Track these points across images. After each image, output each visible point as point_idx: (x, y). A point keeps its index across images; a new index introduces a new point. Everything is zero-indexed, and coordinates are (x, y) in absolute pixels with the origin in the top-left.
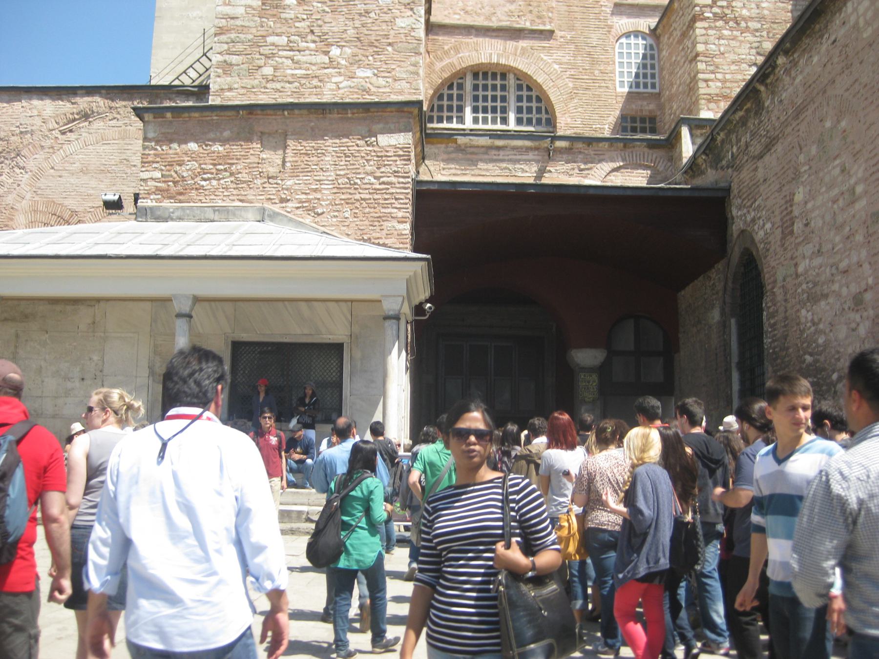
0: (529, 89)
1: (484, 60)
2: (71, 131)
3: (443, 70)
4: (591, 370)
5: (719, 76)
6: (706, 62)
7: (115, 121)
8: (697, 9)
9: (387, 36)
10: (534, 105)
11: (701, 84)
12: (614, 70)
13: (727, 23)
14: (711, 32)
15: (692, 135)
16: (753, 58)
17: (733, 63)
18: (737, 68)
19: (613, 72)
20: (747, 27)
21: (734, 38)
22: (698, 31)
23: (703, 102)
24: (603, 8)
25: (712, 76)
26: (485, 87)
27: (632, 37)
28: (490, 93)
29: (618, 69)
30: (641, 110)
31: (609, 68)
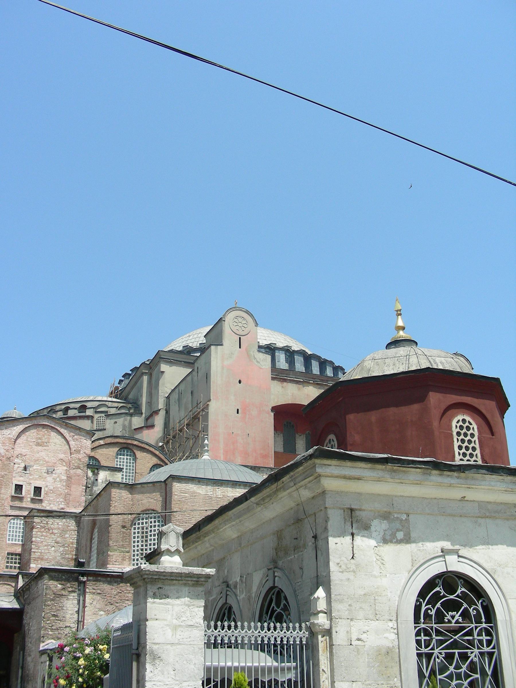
5: (40, 551)
6: (35, 545)
8: (34, 524)
12: (7, 533)
13: (45, 530)
14: (39, 533)
16: (53, 544)
17: (46, 546)
18: (47, 548)
19: (6, 534)
20: (53, 532)
22: (34, 533)
23: (32, 560)
24: (5, 507)
25: (37, 551)
27: (16, 519)
29: (8, 533)
30: (16, 551)
31: (5, 533)
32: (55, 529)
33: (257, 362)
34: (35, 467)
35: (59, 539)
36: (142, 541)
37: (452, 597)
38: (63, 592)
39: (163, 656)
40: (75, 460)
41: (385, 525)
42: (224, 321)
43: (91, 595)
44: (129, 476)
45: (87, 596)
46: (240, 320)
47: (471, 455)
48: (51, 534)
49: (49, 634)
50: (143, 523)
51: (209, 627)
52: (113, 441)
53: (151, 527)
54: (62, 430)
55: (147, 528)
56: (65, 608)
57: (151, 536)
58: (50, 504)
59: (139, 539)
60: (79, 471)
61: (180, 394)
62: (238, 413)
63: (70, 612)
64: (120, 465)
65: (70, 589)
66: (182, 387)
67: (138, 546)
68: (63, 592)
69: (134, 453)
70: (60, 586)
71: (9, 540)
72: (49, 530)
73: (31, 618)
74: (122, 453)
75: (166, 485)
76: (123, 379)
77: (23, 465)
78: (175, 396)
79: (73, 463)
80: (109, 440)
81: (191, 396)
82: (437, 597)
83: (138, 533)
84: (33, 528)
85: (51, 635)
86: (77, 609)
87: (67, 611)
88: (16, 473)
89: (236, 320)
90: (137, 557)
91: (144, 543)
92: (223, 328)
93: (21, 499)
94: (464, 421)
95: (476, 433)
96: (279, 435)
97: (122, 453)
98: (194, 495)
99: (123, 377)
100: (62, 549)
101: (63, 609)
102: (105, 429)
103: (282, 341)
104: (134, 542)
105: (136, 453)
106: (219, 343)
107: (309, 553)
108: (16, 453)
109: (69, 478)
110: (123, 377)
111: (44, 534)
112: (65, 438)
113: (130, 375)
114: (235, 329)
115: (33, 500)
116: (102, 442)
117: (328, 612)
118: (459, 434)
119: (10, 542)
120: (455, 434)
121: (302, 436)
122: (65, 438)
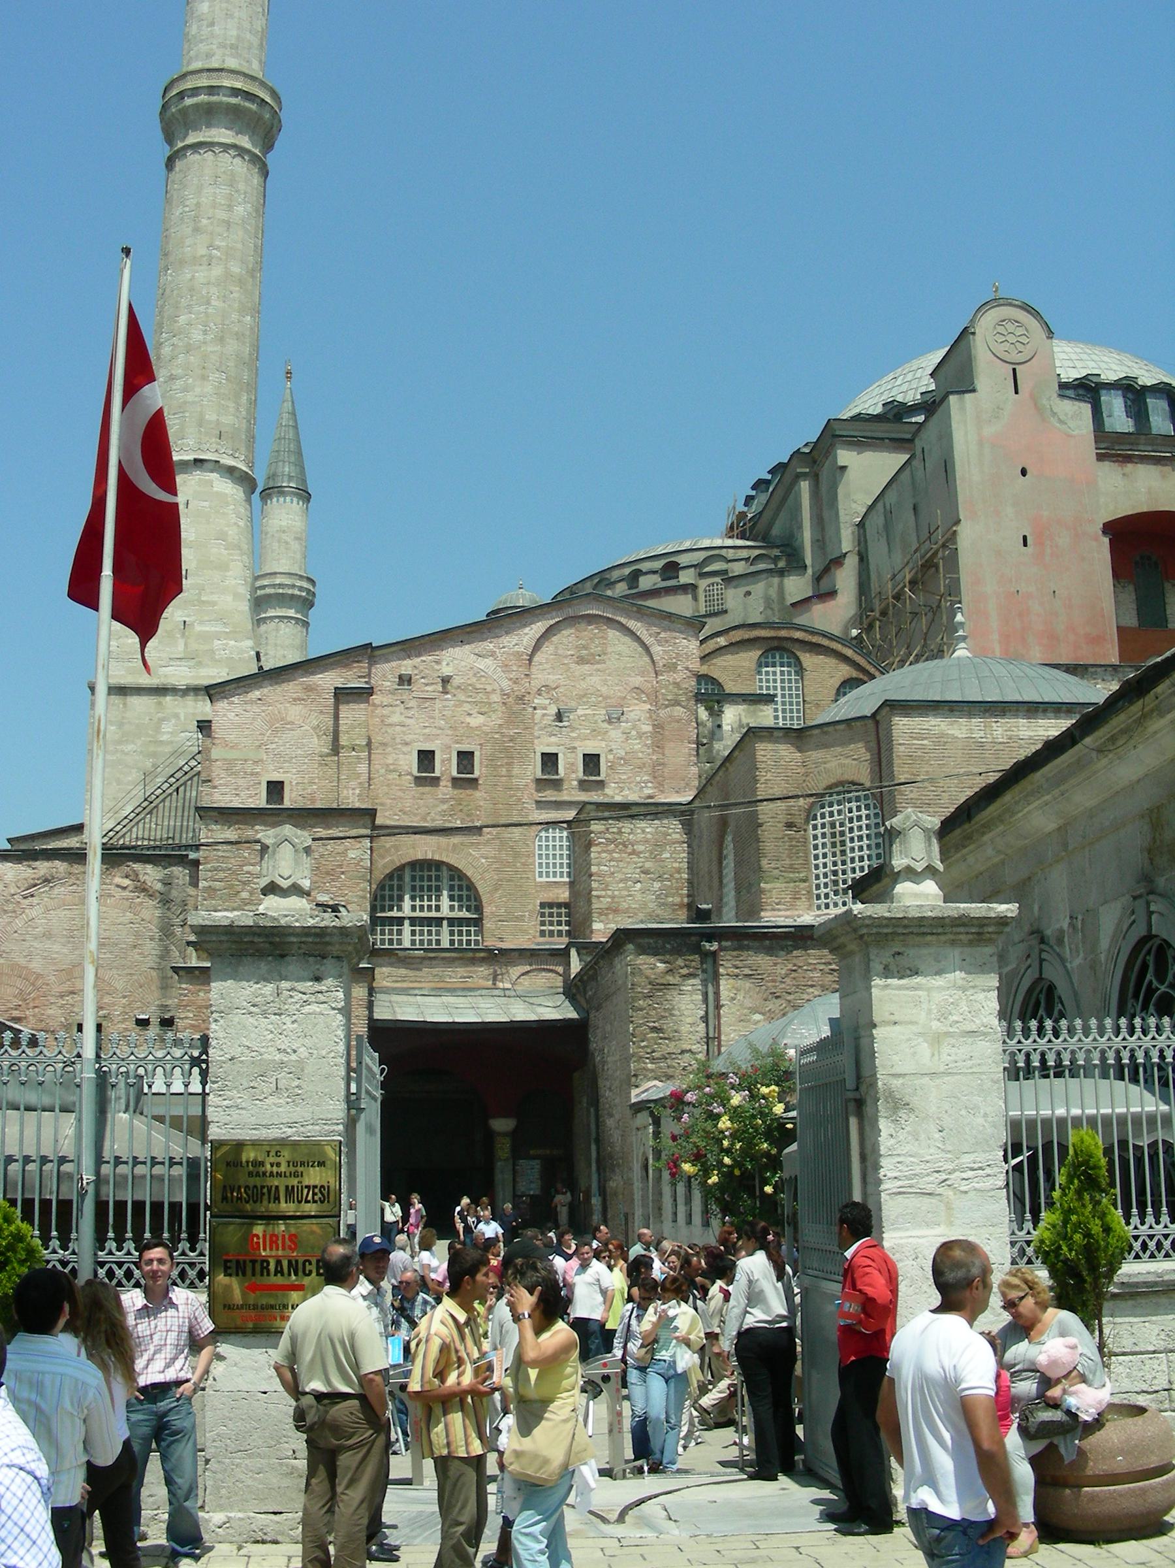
0: (460, 879)
1: (420, 857)
2: (32, 896)
3: (385, 867)
4: (505, 1134)
5: (609, 893)
7: (75, 887)
9: (341, 866)
10: (464, 893)
11: (594, 900)
13: (617, 846)
14: (604, 855)
15: (579, 954)
22: (592, 855)
25: (603, 893)
26: (422, 879)
28: (425, 884)
29: (538, 861)
32: (638, 843)
33: (1061, 421)
34: (580, 712)
35: (648, 865)
36: (834, 855)
38: (670, 979)
39: (915, 1101)
40: (666, 687)
42: (974, 333)
43: (731, 981)
44: (791, 711)
45: (722, 982)
46: (1011, 327)
48: (630, 854)
49: (647, 1070)
50: (831, 814)
51: (1010, 1033)
52: (746, 637)
53: (851, 820)
54: (632, 624)
55: (842, 825)
56: (676, 1012)
57: (852, 840)
58: (622, 789)
59: (826, 850)
60: (679, 711)
61: (888, 514)
62: (1025, 544)
63: (689, 1020)
64: (768, 688)
65: (685, 971)
66: (891, 497)
67: (825, 866)
68: (670, 979)
69: (798, 659)
70: (661, 966)
71: (541, 876)
72: (626, 846)
73: (606, 1038)
74: (770, 660)
75: (877, 723)
76: (753, 493)
77: (553, 710)
78: (877, 520)
79: (663, 694)
80: (737, 636)
83: (824, 835)
84: (589, 845)
85: (652, 1071)
86: (702, 1013)
87: (682, 1018)
88: (541, 729)
89: (1000, 329)
90: (826, 891)
91: (838, 859)
92: (973, 352)
93: (557, 784)
96: (1124, 587)
97: (770, 660)
98: (941, 740)
99: (753, 488)
100: (657, 885)
101: (673, 1015)
102: (726, 612)
103: (1115, 367)
104: (816, 857)
105: (801, 658)
106: (966, 386)
108: (536, 684)
109: (658, 727)
110: (753, 488)
111: (616, 855)
112: (638, 639)
113: (767, 482)
114: (1000, 350)
115: (583, 785)
116: (722, 641)
119: (544, 879)
122: (638, 639)
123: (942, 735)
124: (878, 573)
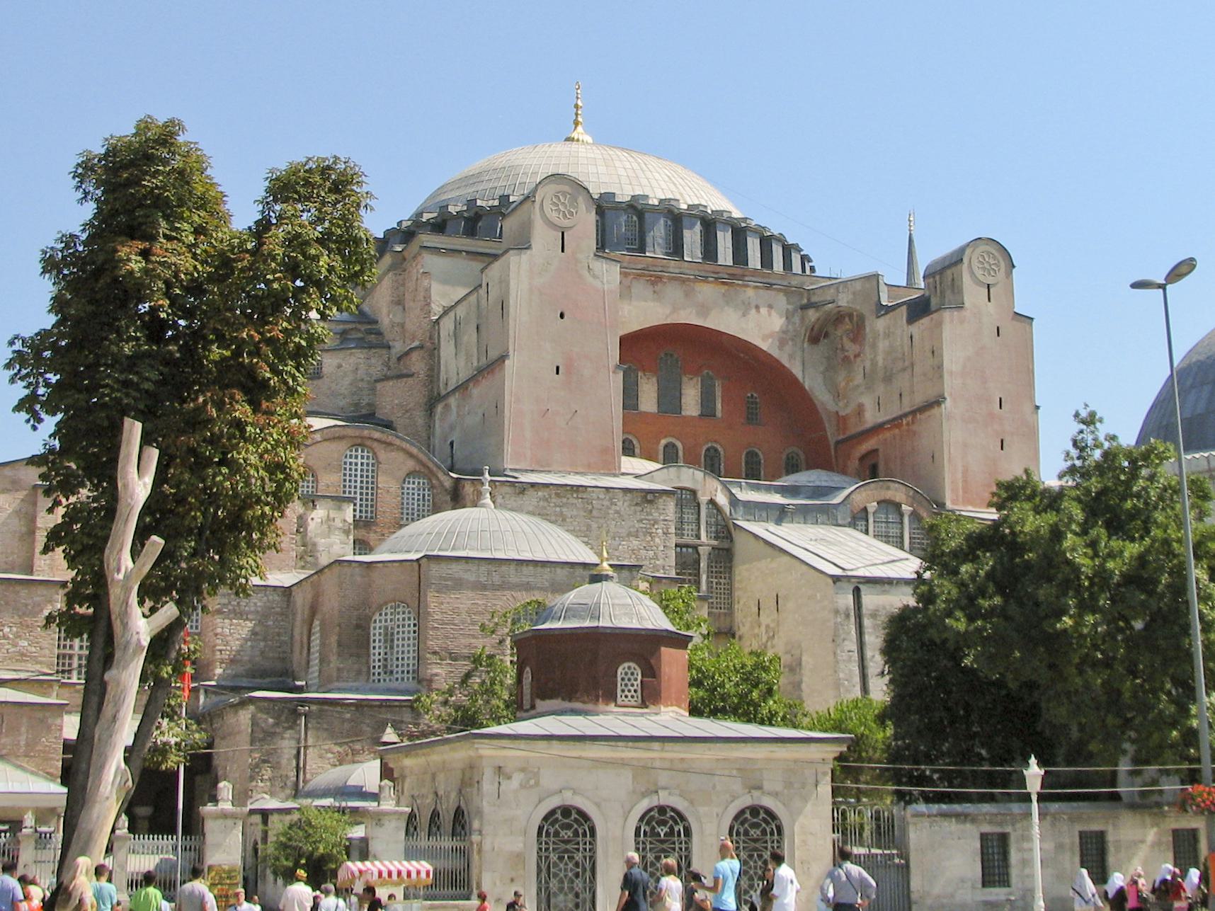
21: (240, 625)
36: (386, 648)
37: (567, 821)
38: (278, 730)
41: (522, 775)
47: (632, 697)
61: (457, 324)
62: (558, 373)
70: (271, 720)
74: (354, 453)
75: (420, 565)
81: (475, 335)
82: (556, 820)
94: (629, 668)
95: (639, 678)
97: (354, 453)
100: (262, 644)
107: (475, 789)
114: (553, 216)
117: (480, 832)
118: (623, 679)
120: (619, 679)
121: (695, 380)
123: (460, 579)
124: (446, 366)
